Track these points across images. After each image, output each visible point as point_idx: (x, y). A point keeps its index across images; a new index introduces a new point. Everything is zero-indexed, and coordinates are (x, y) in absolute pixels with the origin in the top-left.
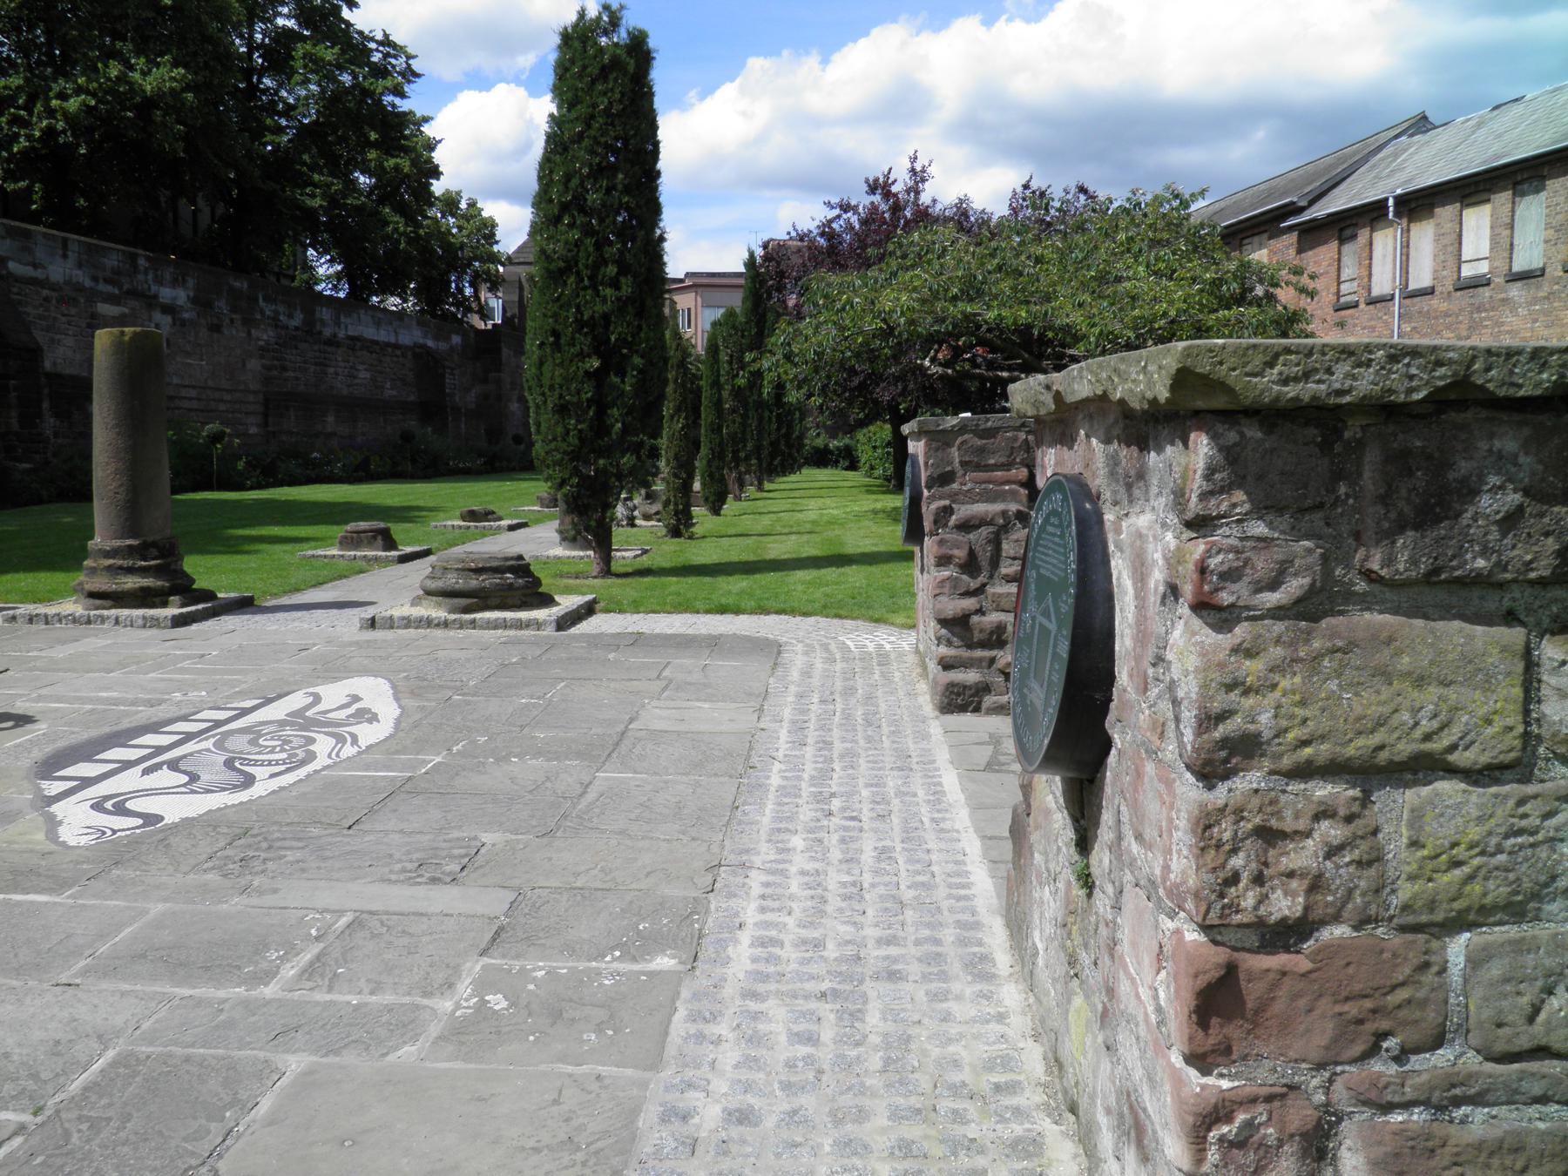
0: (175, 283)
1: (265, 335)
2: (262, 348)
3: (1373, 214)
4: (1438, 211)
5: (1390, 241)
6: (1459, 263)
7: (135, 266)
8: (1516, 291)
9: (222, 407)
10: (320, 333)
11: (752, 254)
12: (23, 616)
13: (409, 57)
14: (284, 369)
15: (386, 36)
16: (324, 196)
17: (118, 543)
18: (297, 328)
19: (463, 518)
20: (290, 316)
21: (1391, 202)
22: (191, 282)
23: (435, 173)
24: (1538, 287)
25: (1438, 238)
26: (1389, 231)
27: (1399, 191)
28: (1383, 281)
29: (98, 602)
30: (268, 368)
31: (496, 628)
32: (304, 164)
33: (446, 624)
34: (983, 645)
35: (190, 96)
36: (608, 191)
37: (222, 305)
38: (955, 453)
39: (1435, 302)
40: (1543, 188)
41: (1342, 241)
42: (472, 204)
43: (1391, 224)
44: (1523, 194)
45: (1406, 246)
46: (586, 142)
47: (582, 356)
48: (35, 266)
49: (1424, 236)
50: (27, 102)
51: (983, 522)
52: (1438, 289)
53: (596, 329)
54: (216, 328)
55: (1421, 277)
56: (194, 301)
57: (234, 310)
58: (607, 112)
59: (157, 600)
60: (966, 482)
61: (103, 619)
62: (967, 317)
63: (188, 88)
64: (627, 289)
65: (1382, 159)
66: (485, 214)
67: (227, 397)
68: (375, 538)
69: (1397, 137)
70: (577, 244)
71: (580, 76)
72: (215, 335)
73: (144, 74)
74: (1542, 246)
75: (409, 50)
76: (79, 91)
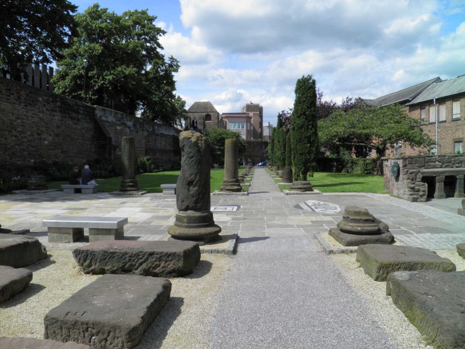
1: (146, 133)
2: (145, 137)
3: (430, 103)
4: (446, 102)
5: (434, 109)
6: (452, 115)
7: (123, 117)
11: (279, 114)
13: (178, 62)
14: (149, 142)
15: (172, 57)
16: (159, 98)
17: (232, 180)
20: (150, 128)
21: (434, 100)
22: (133, 120)
25: (447, 109)
26: (434, 107)
27: (436, 97)
28: (433, 119)
32: (153, 89)
33: (302, 194)
34: (417, 191)
36: (311, 111)
37: (138, 126)
38: (407, 162)
39: (446, 124)
41: (421, 109)
42: (179, 97)
43: (434, 105)
45: (438, 110)
46: (306, 102)
47: (306, 144)
48: (106, 117)
49: (443, 109)
50: (97, 77)
51: (414, 172)
52: (447, 121)
53: (309, 138)
54: (137, 132)
55: (443, 118)
57: (140, 127)
58: (310, 96)
60: (409, 166)
61: (233, 194)
62: (353, 132)
63: (136, 73)
64: (314, 131)
65: (430, 89)
66: (183, 100)
67: (139, 149)
69: (433, 83)
70: (304, 122)
71: (304, 89)
75: (178, 61)
76: (111, 74)
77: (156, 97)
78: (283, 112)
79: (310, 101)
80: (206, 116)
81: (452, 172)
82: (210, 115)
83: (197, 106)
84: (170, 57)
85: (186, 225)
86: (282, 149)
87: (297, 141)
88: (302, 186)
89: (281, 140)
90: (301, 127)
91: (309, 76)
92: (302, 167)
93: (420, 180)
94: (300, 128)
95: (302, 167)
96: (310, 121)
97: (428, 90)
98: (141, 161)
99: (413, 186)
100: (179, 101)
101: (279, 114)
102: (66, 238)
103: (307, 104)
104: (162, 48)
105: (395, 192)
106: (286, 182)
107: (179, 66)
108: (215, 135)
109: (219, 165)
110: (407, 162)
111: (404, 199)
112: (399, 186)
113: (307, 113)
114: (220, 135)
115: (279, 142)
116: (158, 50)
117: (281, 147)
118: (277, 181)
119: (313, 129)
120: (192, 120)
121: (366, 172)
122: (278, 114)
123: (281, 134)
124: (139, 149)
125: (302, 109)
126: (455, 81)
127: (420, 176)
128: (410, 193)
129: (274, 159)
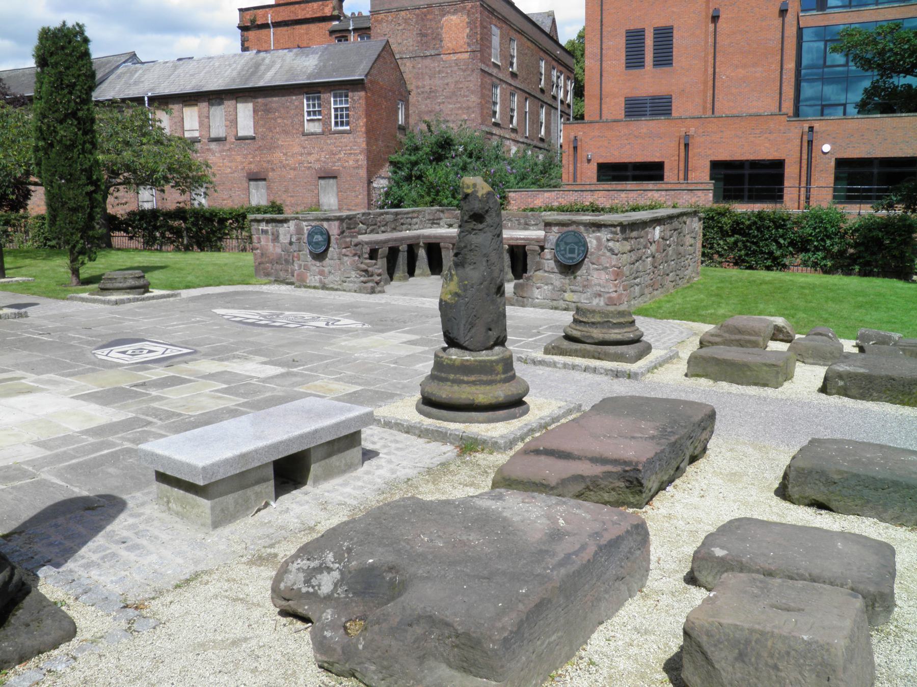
6: (183, 131)
8: (213, 146)
21: (146, 99)
24: (224, 145)
27: (150, 94)
40: (223, 103)
44: (213, 105)
46: (78, 88)
47: (85, 185)
69: (124, 62)
70: (76, 134)
74: (224, 128)
81: (396, 240)
85: (503, 376)
91: (78, 24)
93: (367, 256)
97: (119, 77)
99: (363, 266)
102: (258, 496)
103: (81, 92)
105: (314, 280)
110: (345, 225)
111: (344, 290)
112: (326, 270)
113: (80, 114)
126: (175, 67)
127: (367, 249)
128: (362, 279)
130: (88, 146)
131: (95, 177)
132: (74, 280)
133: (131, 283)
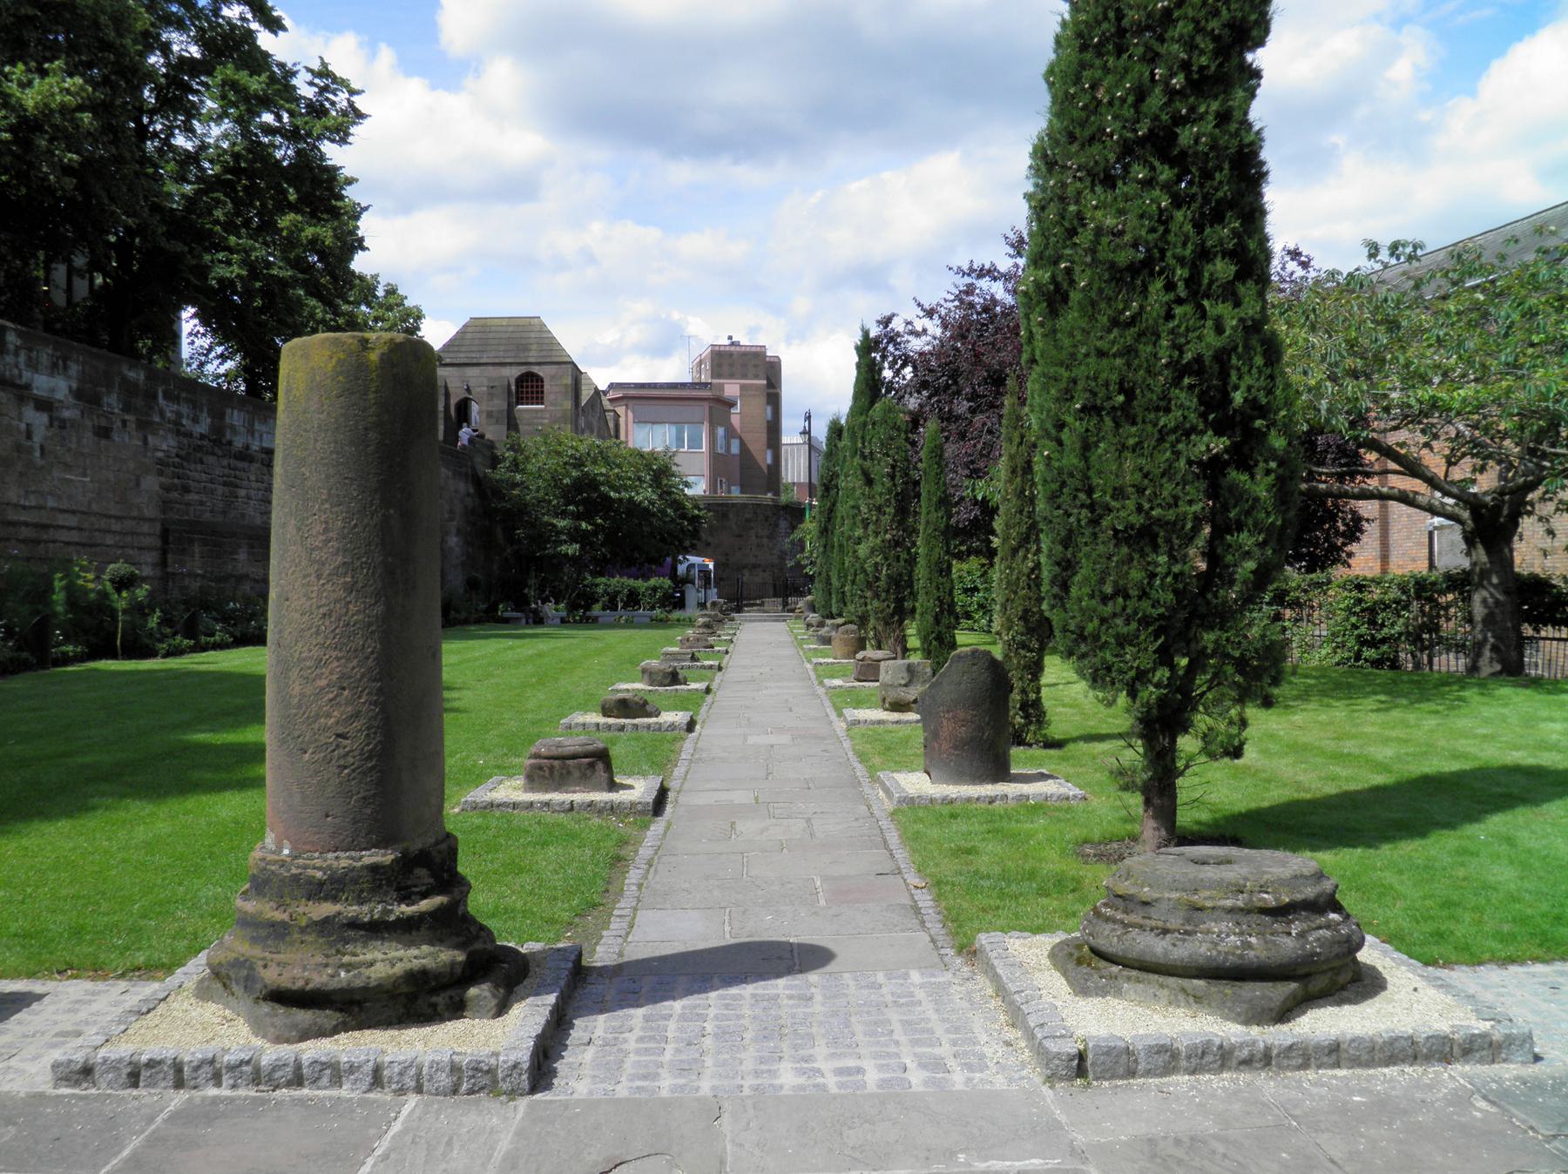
0: (54, 369)
1: (165, 443)
2: (160, 462)
9: (109, 540)
10: (230, 443)
11: (866, 333)
12: (113, 1066)
13: (352, 92)
14: (186, 489)
15: (324, 65)
16: (245, 263)
17: (343, 861)
18: (202, 437)
19: (606, 712)
20: (195, 420)
22: (74, 369)
23: (359, 245)
29: (304, 1016)
30: (167, 489)
31: (1391, 1060)
32: (217, 222)
35: (86, 117)
37: (112, 401)
42: (391, 291)
46: (1182, 28)
54: (104, 433)
56: (78, 394)
57: (127, 408)
59: (440, 999)
67: (116, 526)
68: (592, 766)
70: (1164, 219)
72: (103, 442)
73: (24, 85)
75: (354, 86)
77: (229, 263)
78: (886, 322)
79: (1214, 25)
80: (520, 380)
82: (539, 379)
83: (479, 336)
84: (316, 66)
86: (886, 519)
87: (1090, 410)
88: (1257, 946)
89: (881, 469)
90: (1134, 269)
92: (1146, 662)
94: (1131, 276)
95: (1146, 662)
96: (1218, 218)
98: (74, 596)
100: (390, 308)
101: (866, 333)
103: (1191, 46)
104: (275, 25)
106: (959, 777)
107: (360, 115)
108: (552, 463)
109: (573, 607)
113: (1185, 136)
114: (579, 463)
115: (869, 482)
116: (265, 40)
117: (879, 509)
118: (880, 751)
119: (1247, 290)
120: (453, 401)
121: (1369, 653)
122: (857, 338)
123: (882, 432)
124: (116, 526)
125: (1141, 95)
129: (835, 582)
130: (1222, 269)
131: (1238, 398)
132: (1150, 830)
133: (1225, 940)
